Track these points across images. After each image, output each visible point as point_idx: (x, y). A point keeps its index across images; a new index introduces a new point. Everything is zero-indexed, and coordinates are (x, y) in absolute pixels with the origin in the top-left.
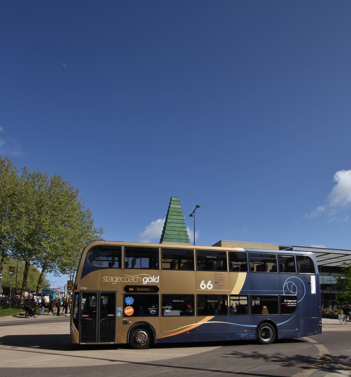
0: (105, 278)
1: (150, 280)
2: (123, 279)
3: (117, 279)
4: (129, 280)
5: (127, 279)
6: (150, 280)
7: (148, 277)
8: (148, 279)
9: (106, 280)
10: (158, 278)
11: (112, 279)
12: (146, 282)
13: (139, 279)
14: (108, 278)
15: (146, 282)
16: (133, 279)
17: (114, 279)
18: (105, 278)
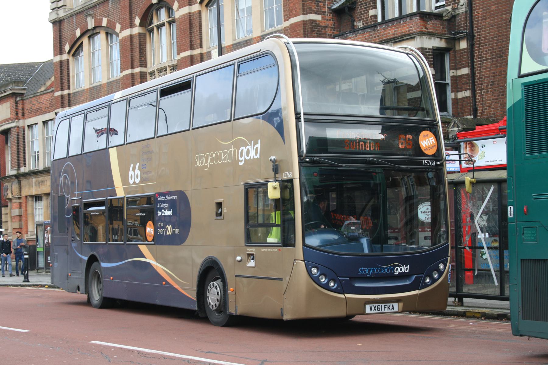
0: (361, 270)
1: (401, 270)
2: (377, 270)
3: (372, 270)
4: (382, 271)
5: (381, 270)
6: (401, 270)
7: (400, 266)
8: (399, 269)
9: (361, 272)
10: (408, 267)
11: (367, 270)
12: (398, 272)
13: (392, 269)
14: (363, 270)
15: (398, 272)
16: (386, 270)
17: (369, 271)
18: (361, 270)
